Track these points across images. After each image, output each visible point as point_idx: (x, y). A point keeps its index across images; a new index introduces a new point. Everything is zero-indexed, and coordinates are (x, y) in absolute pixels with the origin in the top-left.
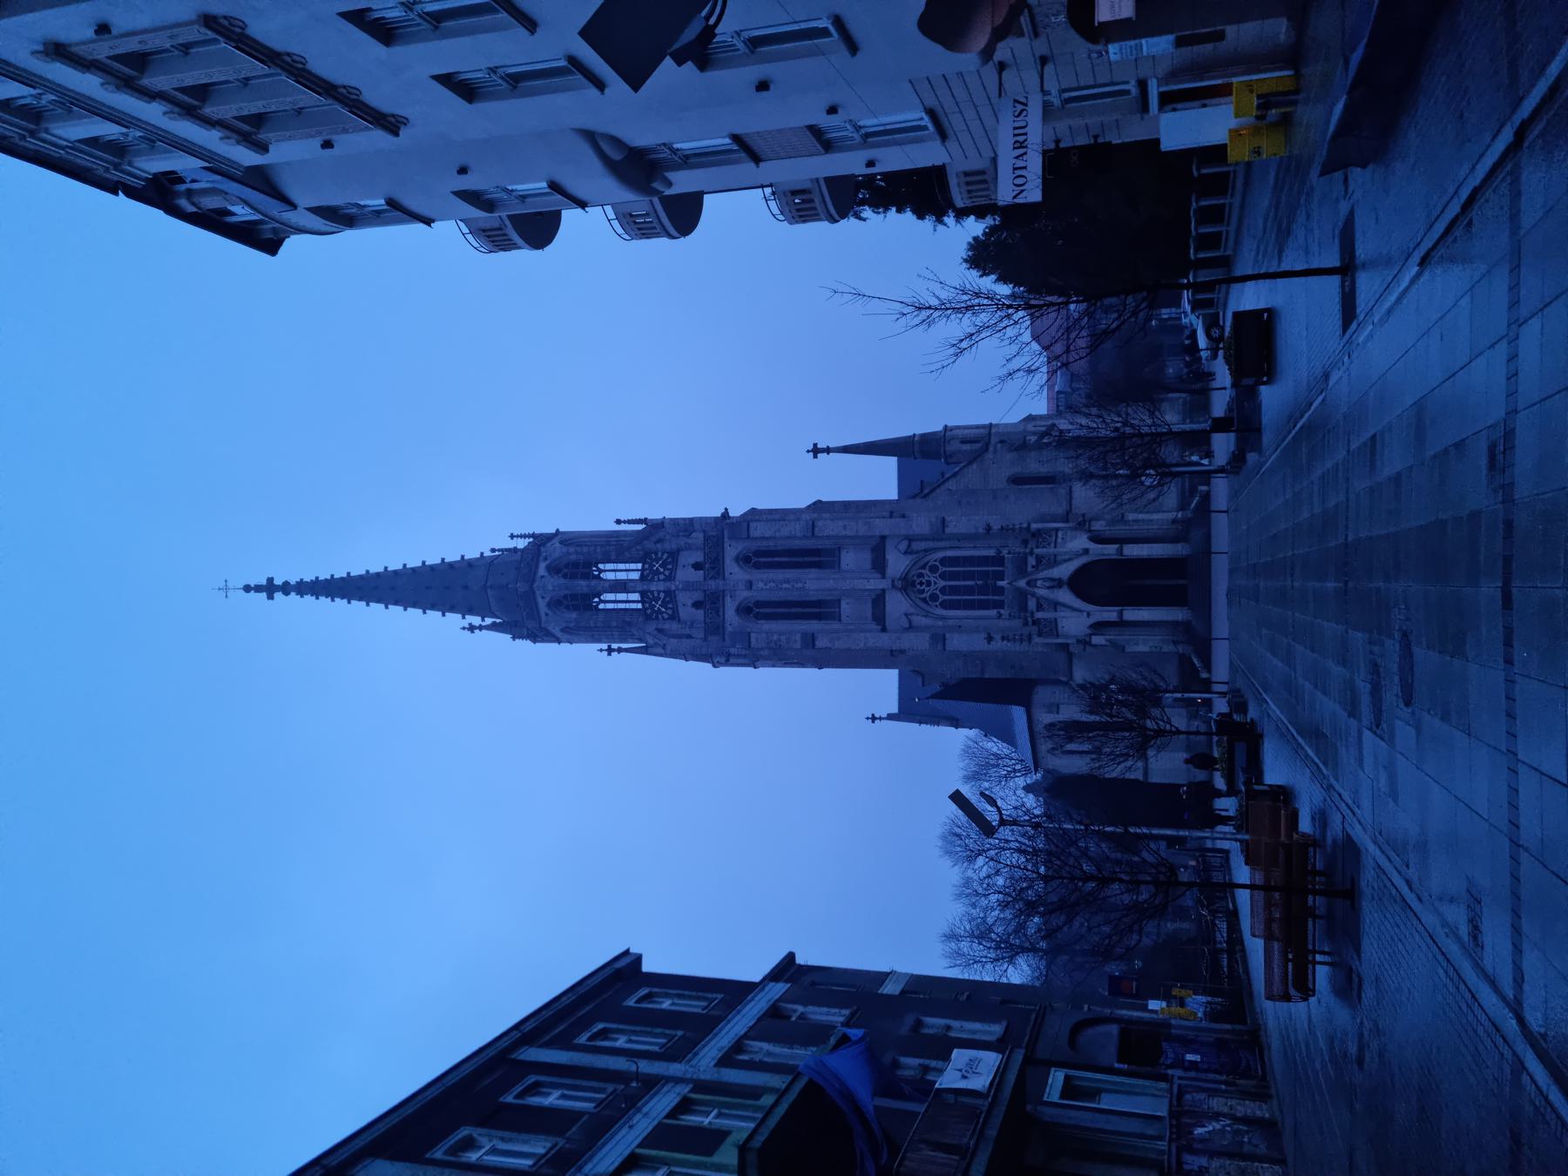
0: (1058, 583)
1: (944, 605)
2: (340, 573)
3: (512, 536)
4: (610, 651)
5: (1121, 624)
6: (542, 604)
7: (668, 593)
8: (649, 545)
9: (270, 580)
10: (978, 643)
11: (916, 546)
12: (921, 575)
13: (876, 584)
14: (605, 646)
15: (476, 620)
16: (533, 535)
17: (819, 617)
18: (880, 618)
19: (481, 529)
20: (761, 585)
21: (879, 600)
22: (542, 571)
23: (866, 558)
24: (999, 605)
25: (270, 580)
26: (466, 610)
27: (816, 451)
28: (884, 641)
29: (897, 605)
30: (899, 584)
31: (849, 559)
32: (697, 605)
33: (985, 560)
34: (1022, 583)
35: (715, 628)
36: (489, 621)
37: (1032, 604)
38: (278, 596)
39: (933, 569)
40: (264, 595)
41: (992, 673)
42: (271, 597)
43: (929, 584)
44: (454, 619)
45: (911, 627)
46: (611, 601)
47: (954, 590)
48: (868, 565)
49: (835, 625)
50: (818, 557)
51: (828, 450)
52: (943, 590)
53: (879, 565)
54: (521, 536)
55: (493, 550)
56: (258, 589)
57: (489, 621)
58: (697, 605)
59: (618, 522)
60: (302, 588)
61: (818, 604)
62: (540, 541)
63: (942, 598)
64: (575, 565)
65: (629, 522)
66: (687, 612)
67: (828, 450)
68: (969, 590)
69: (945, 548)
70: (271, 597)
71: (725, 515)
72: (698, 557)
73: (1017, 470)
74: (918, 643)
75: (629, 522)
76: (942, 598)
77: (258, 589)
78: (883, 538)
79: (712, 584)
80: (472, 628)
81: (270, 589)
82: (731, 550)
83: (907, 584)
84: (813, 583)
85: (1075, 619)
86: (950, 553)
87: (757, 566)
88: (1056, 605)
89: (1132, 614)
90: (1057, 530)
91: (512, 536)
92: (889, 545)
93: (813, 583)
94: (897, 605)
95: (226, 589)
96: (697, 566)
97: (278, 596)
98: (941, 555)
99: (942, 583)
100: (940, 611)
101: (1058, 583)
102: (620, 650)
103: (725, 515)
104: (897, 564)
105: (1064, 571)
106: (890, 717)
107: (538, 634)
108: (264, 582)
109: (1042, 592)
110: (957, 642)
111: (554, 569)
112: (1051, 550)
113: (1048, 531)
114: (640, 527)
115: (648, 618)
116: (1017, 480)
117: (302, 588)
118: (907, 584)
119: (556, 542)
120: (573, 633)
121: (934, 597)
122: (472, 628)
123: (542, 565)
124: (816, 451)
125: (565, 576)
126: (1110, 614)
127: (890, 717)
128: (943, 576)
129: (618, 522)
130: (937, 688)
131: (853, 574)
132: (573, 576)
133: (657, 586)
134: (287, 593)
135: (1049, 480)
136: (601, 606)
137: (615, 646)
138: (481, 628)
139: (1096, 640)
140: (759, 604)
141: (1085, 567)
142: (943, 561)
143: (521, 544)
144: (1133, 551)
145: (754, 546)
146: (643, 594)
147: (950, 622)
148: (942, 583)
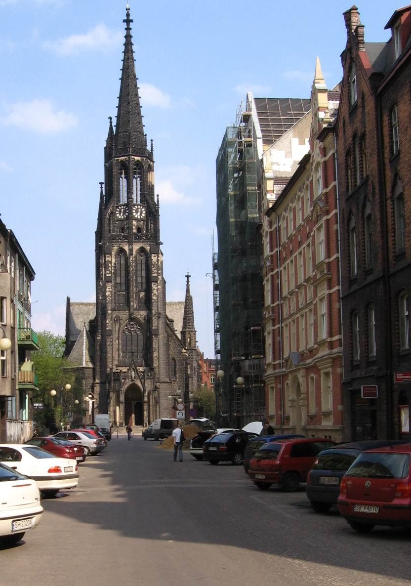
2: (135, 56)
3: (152, 140)
9: (132, 21)
14: (103, 181)
15: (114, 123)
16: (152, 153)
25: (132, 21)
26: (118, 117)
27: (188, 277)
29: (124, 315)
36: (114, 129)
40: (126, 18)
42: (124, 21)
44: (114, 113)
51: (188, 282)
54: (152, 146)
55: (146, 135)
56: (128, 15)
57: (114, 129)
59: (158, 196)
60: (128, 37)
62: (150, 157)
65: (158, 200)
67: (188, 282)
70: (124, 21)
75: (158, 200)
77: (128, 15)
81: (128, 21)
91: (152, 140)
96: (139, 229)
102: (102, 188)
108: (131, 18)
117: (128, 37)
124: (188, 277)
129: (158, 196)
134: (126, 29)
137: (103, 186)
138: (111, 122)
143: (149, 148)
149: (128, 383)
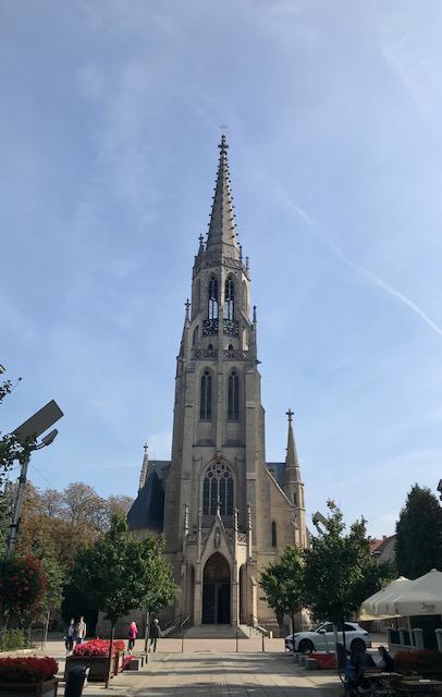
0: (217, 544)
1: (206, 480)
4: (187, 304)
5: (193, 583)
6: (213, 270)
7: (217, 332)
8: (242, 323)
9: (227, 147)
10: (185, 499)
11: (239, 464)
12: (223, 467)
13: (219, 442)
15: (205, 240)
17: (202, 412)
18: (199, 444)
19: (248, 241)
20: (220, 379)
21: (211, 443)
22: (230, 271)
23: (233, 437)
24: (205, 512)
25: (227, 147)
26: (210, 235)
28: (187, 446)
29: (207, 454)
30: (219, 454)
31: (233, 427)
32: (211, 347)
33: (231, 504)
34: (217, 524)
35: (197, 356)
37: (206, 530)
38: (220, 150)
39: (226, 475)
41: (167, 507)
42: (219, 146)
43: (218, 472)
45: (194, 461)
46: (213, 306)
47: (214, 485)
48: (230, 438)
49: (197, 417)
50: (236, 411)
51: (290, 420)
52: (215, 479)
53: (228, 444)
56: (223, 141)
58: (211, 347)
59: (255, 308)
61: (209, 411)
63: (210, 479)
64: (232, 287)
66: (207, 341)
67: (290, 420)
68: (214, 496)
69: (238, 480)
70: (219, 146)
71: (258, 362)
72: (235, 347)
73: (279, 523)
74: (186, 465)
76: (210, 479)
77: (223, 141)
78: (245, 446)
79: (221, 356)
80: (201, 238)
82: (238, 365)
83: (218, 460)
84: (221, 407)
85: (199, 557)
86: (235, 482)
87: (230, 378)
88: (204, 544)
89: (199, 589)
90: (248, 546)
92: (241, 449)
93: (221, 407)
94: (207, 454)
95: (224, 127)
96: (230, 347)
97: (220, 150)
98: (234, 478)
99: (219, 479)
100: (203, 479)
101: (217, 544)
103: (258, 362)
104: (230, 454)
105: (224, 550)
106: (146, 456)
107: (197, 268)
108: (226, 143)
109: (212, 536)
110: (185, 486)
111: (230, 277)
112: (237, 542)
113: (247, 541)
114: (251, 320)
115: (205, 322)
116: (274, 524)
118: (218, 460)
119: (244, 278)
120: (197, 286)
121: (211, 474)
122: (201, 238)
123: (233, 271)
124: (290, 414)
125: (227, 281)
126: (199, 576)
127: (146, 456)
128: (222, 480)
129: (255, 308)
130: (160, 477)
131: (223, 429)
132: (227, 286)
133: (221, 327)
135: (274, 544)
136: (211, 302)
139: (184, 567)
140: (210, 378)
141: (226, 561)
142: (231, 480)
144: (236, 591)
145: (240, 377)
146: (217, 320)
147: (197, 483)
148: (219, 479)
149: (210, 551)
